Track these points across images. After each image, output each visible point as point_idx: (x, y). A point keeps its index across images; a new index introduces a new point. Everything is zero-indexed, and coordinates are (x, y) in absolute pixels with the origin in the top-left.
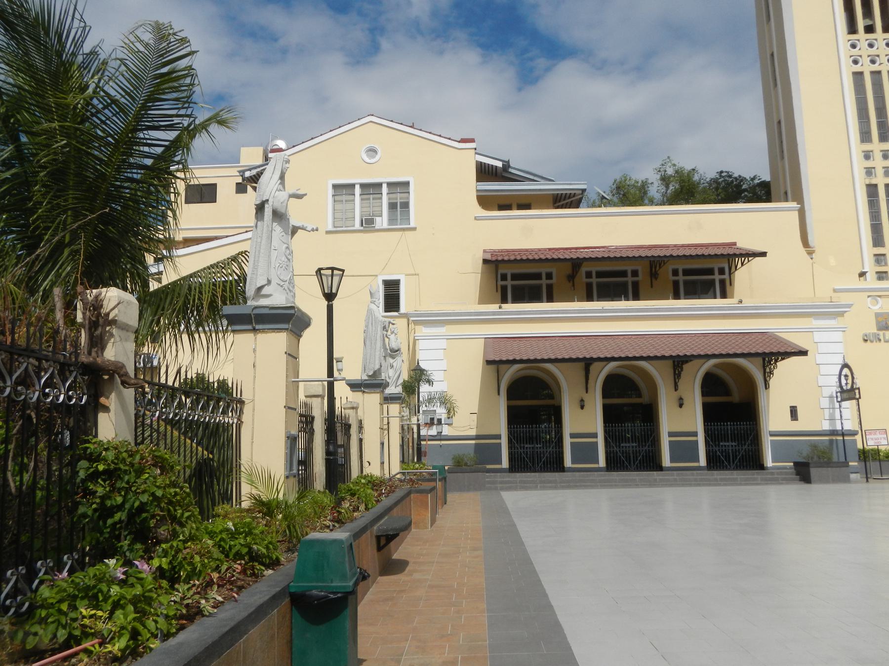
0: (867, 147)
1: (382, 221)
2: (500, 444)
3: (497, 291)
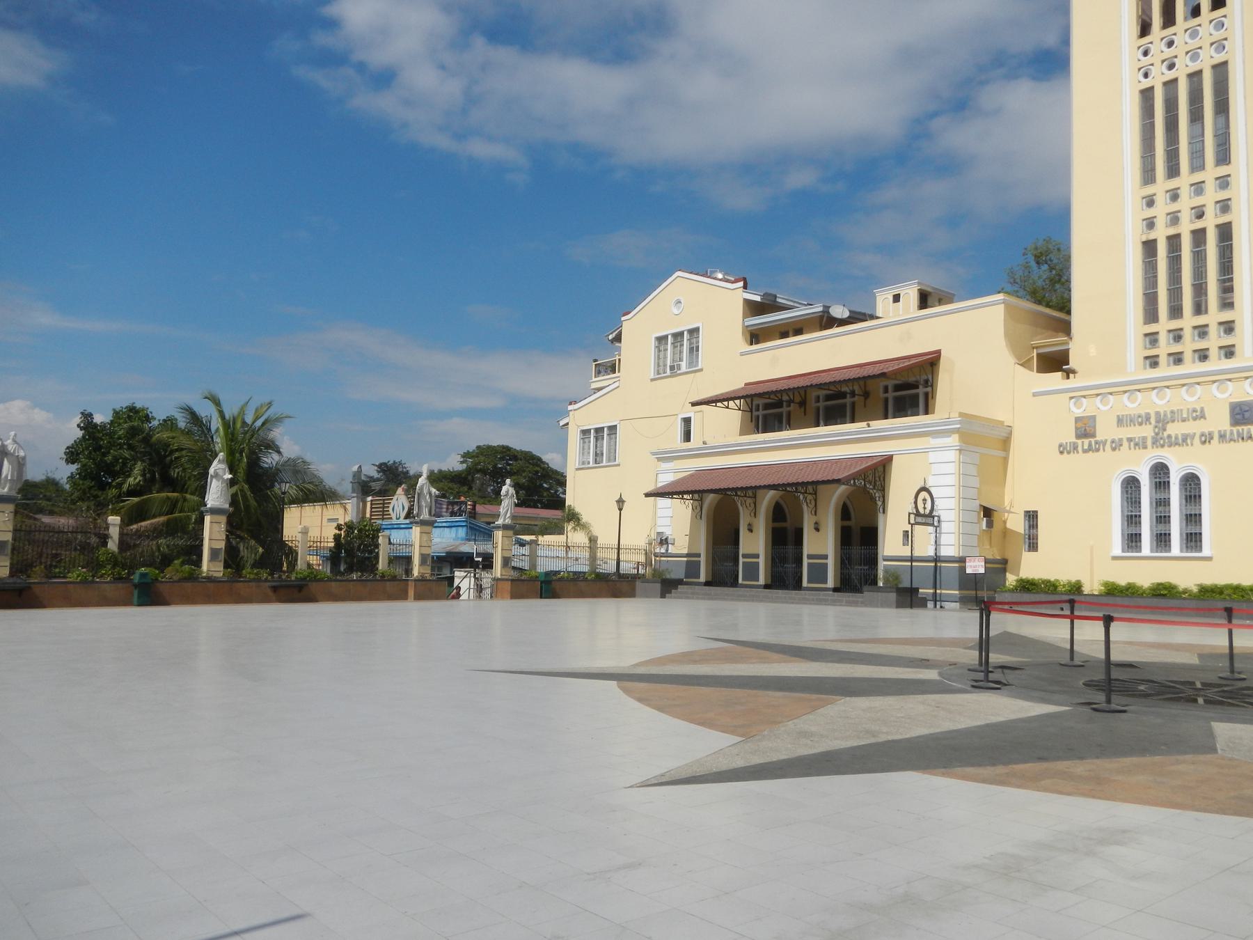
0: (1149, 190)
1: (684, 364)
2: (700, 561)
3: (752, 421)
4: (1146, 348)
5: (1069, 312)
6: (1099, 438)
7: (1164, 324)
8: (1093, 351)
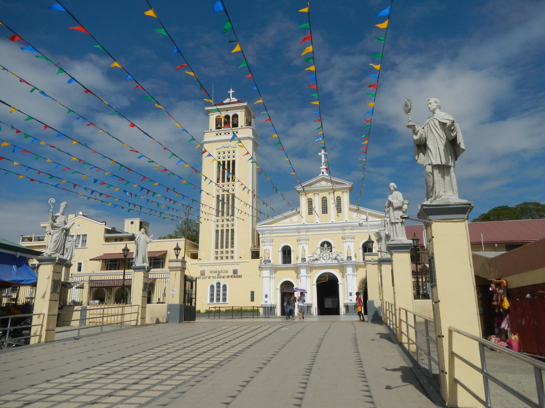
1: (80, 246)
4: (215, 255)
5: (198, 243)
6: (205, 276)
7: (219, 250)
8: (204, 254)
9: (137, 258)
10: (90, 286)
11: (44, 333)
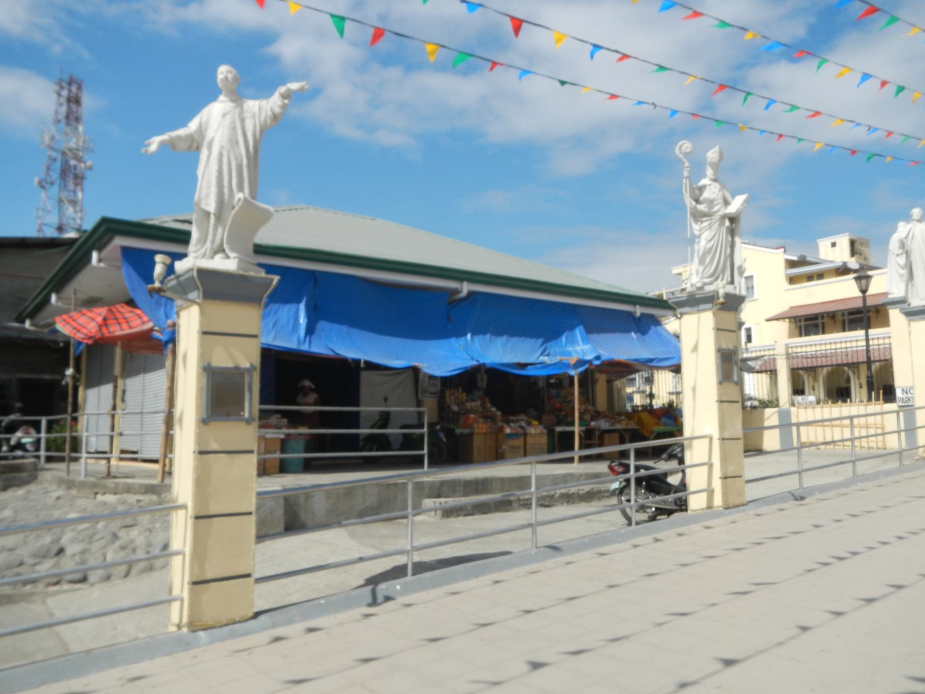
3: (796, 327)
9: (912, 285)
10: (792, 367)
11: (717, 484)
